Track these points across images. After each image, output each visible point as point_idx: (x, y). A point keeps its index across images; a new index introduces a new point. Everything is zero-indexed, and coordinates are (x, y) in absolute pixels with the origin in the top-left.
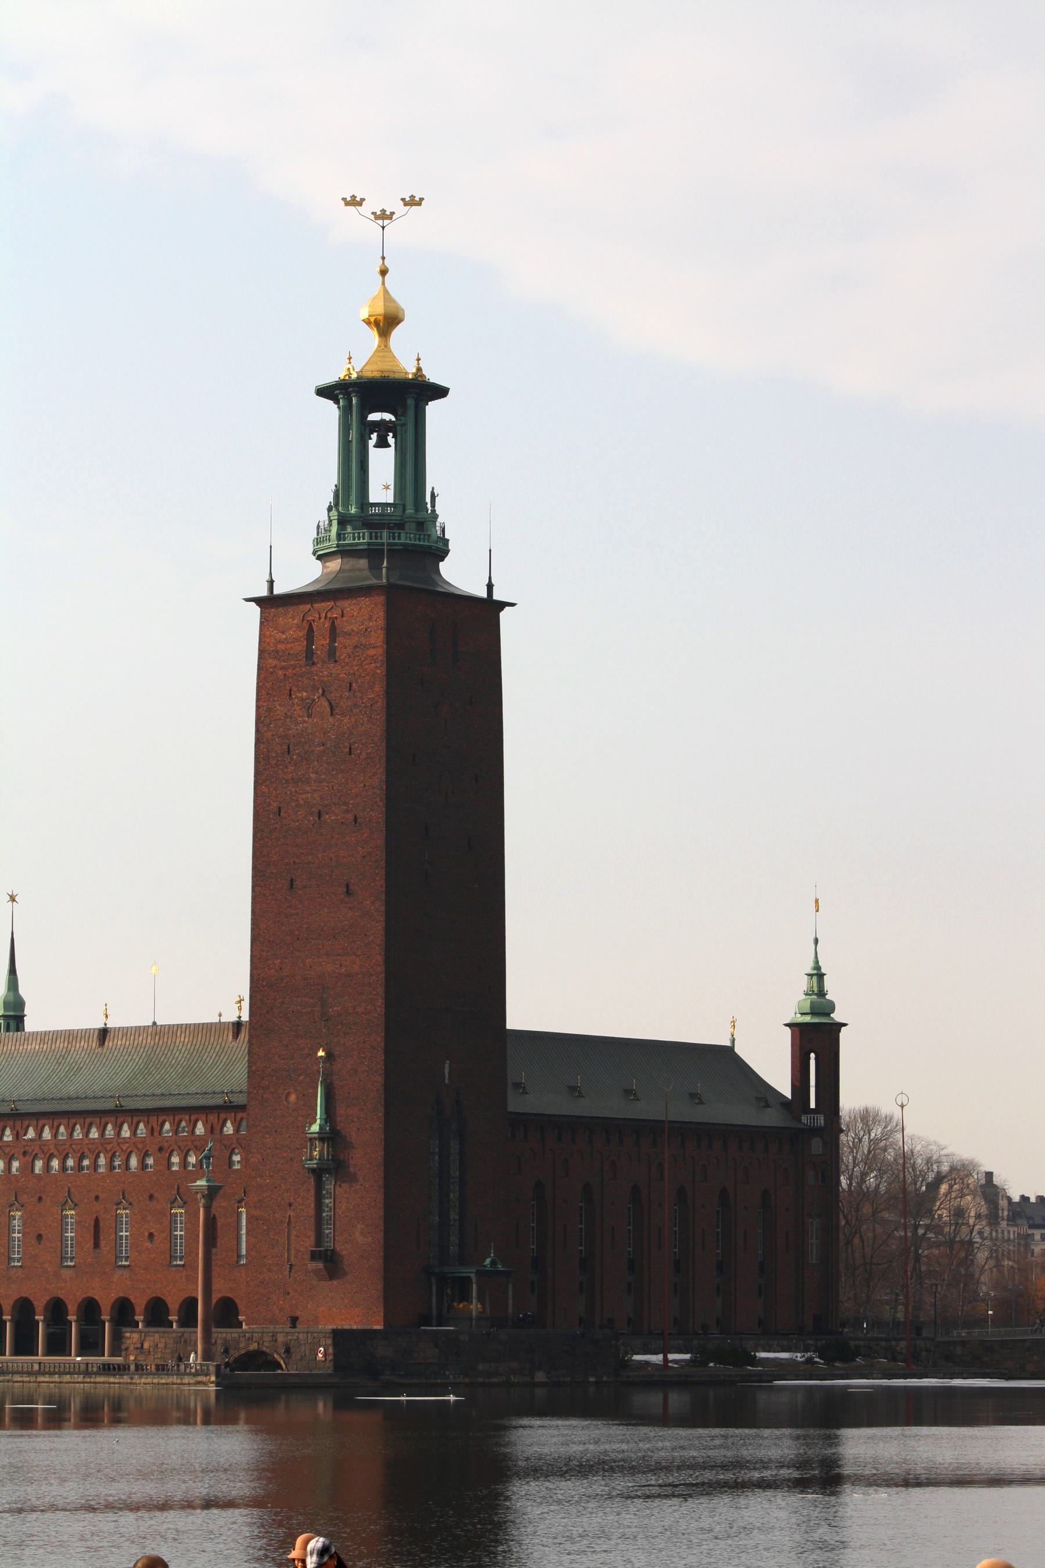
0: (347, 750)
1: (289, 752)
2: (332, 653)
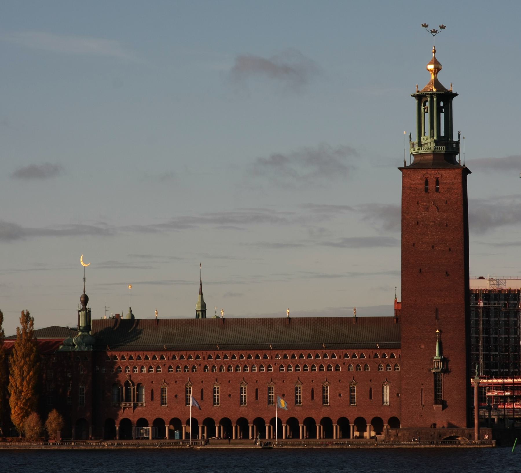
0: (446, 225)
1: (418, 224)
2: (437, 190)
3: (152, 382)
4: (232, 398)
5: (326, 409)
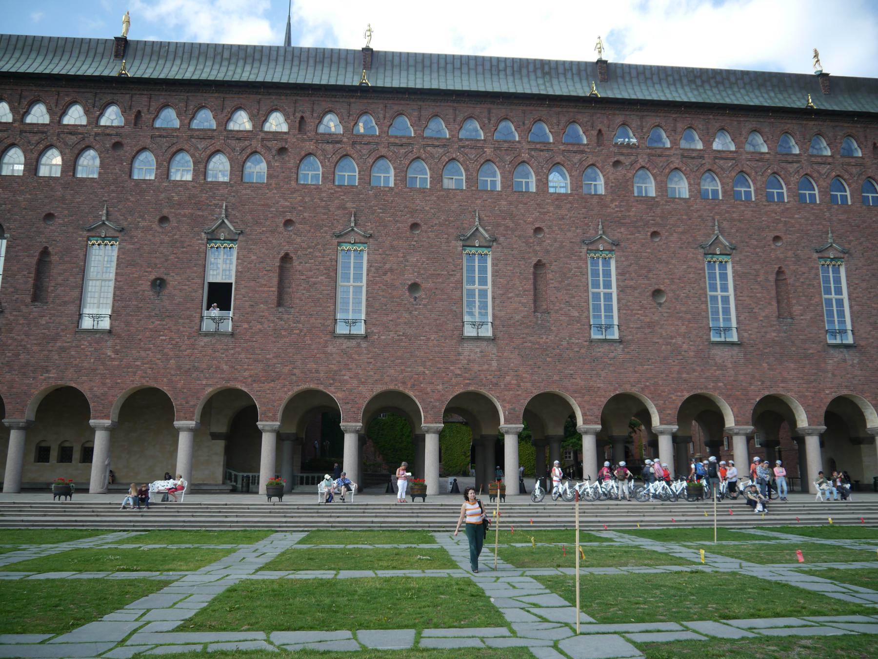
3: (49, 216)
4: (425, 302)
5: (845, 360)
